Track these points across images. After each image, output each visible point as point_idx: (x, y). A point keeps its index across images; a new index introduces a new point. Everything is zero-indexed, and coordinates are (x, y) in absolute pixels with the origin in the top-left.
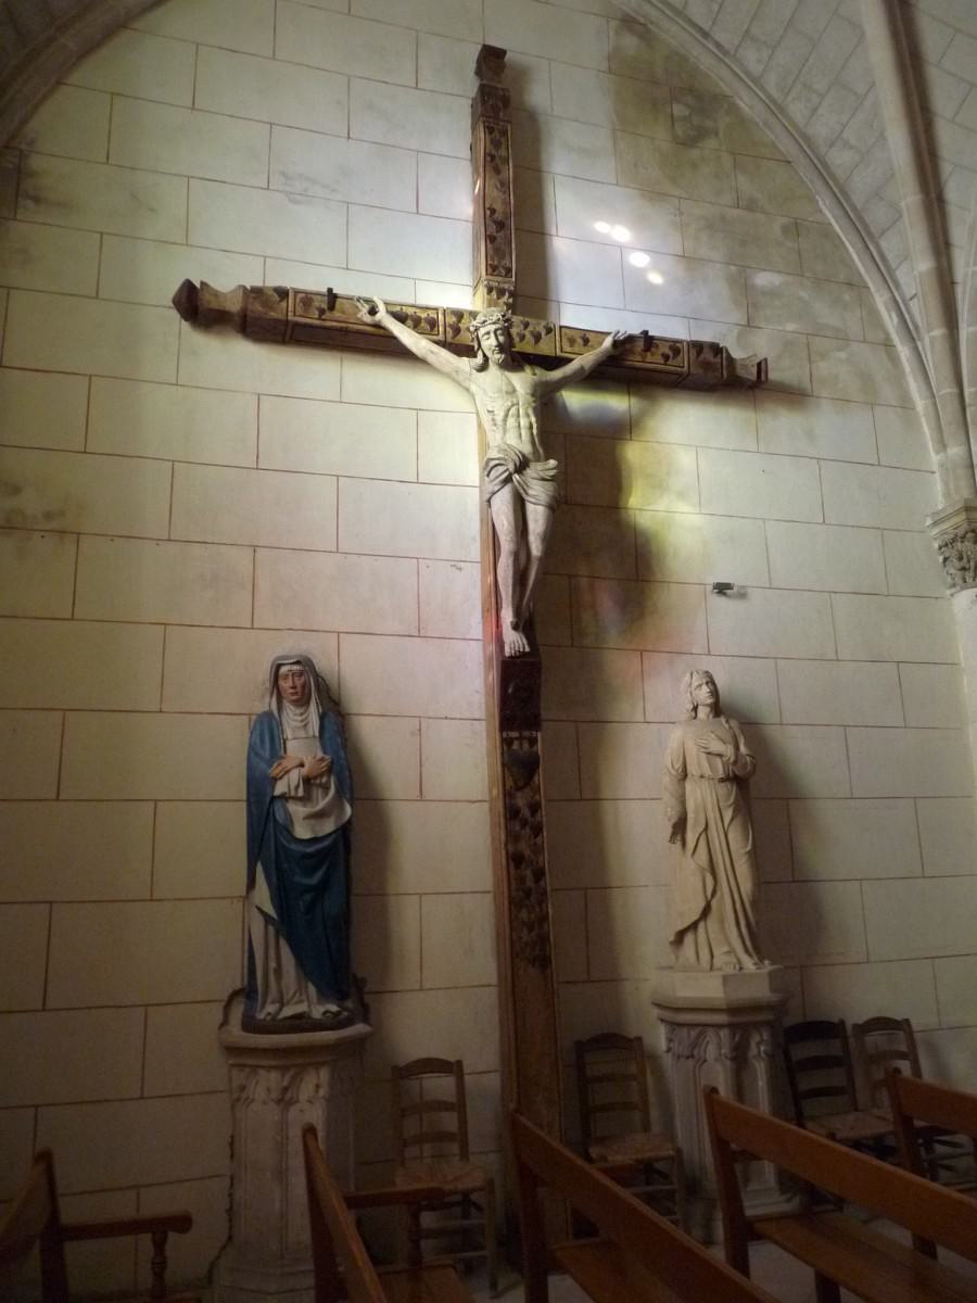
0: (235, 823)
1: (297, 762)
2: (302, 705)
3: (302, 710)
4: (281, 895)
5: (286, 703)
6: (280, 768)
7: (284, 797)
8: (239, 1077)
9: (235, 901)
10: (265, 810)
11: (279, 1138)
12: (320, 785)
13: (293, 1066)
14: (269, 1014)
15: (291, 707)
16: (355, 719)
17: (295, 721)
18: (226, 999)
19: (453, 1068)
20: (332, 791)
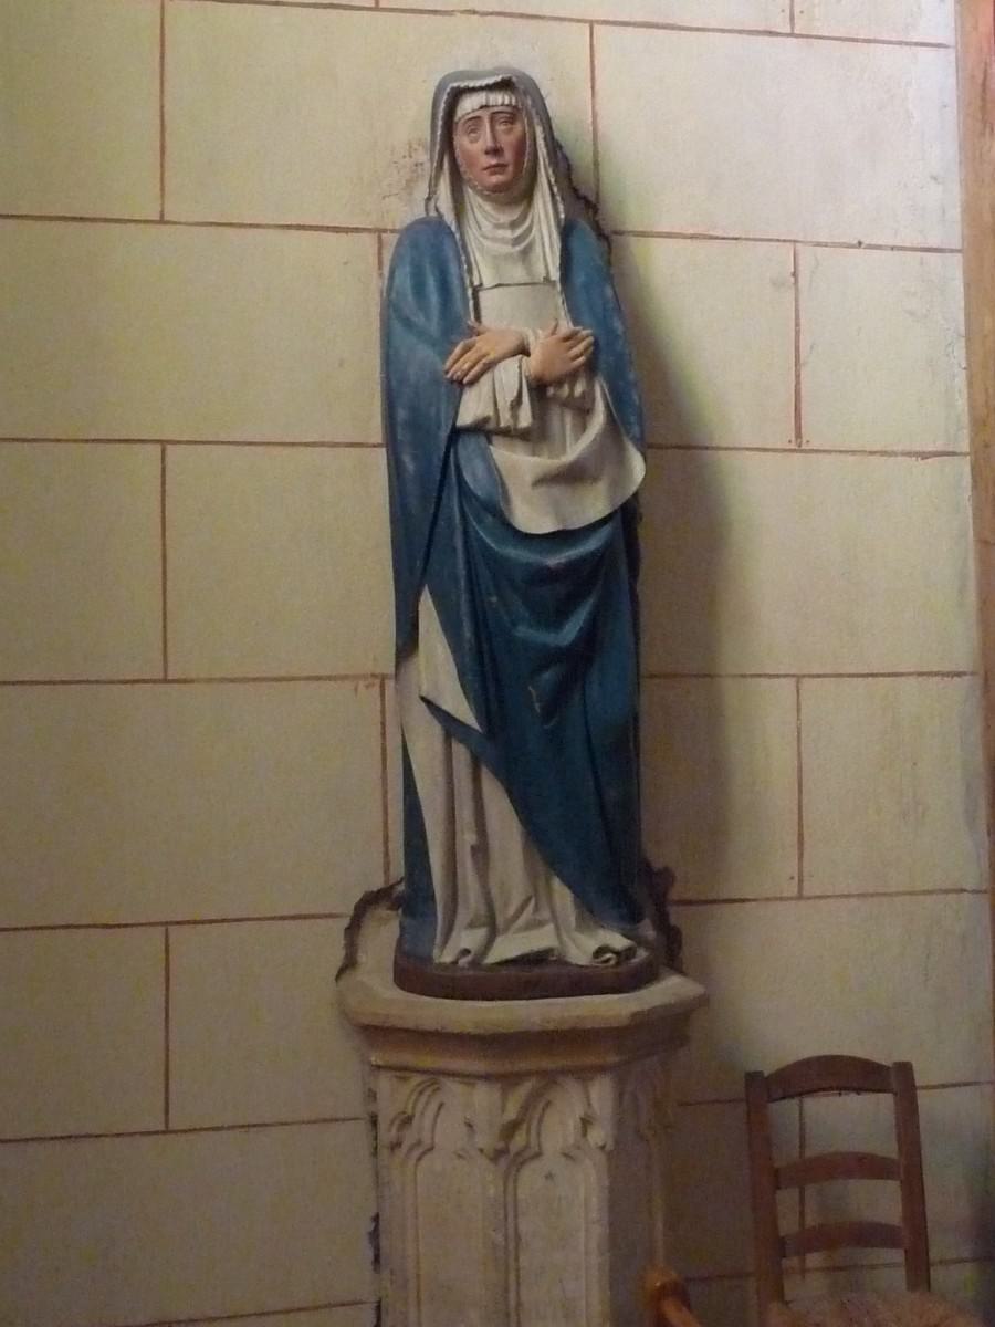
0: (360, 500)
1: (511, 343)
2: (511, 202)
3: (515, 214)
4: (485, 667)
5: (473, 199)
6: (471, 356)
7: (483, 430)
8: (393, 1096)
9: (361, 684)
10: (437, 463)
11: (499, 1238)
12: (567, 403)
13: (528, 1074)
14: (466, 952)
15: (488, 207)
16: (636, 247)
17: (494, 240)
18: (351, 911)
19: (895, 1080)
20: (598, 420)
